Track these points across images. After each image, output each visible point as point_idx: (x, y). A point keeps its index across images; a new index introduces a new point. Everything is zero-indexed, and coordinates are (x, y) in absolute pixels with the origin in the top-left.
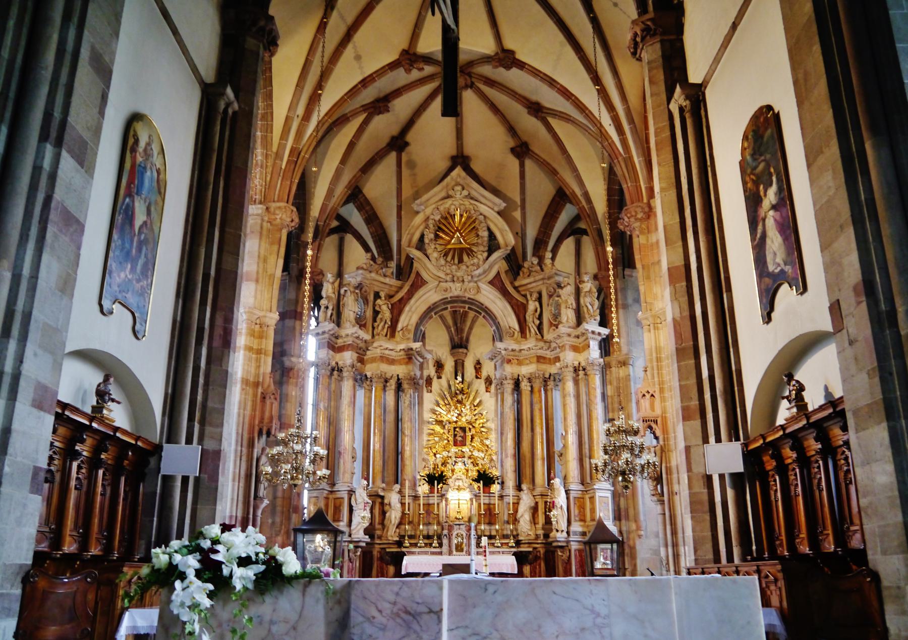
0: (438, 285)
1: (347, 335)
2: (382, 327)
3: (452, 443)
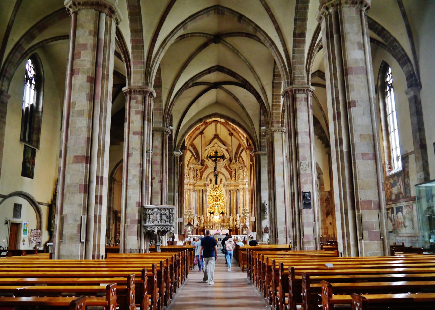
2: (198, 178)
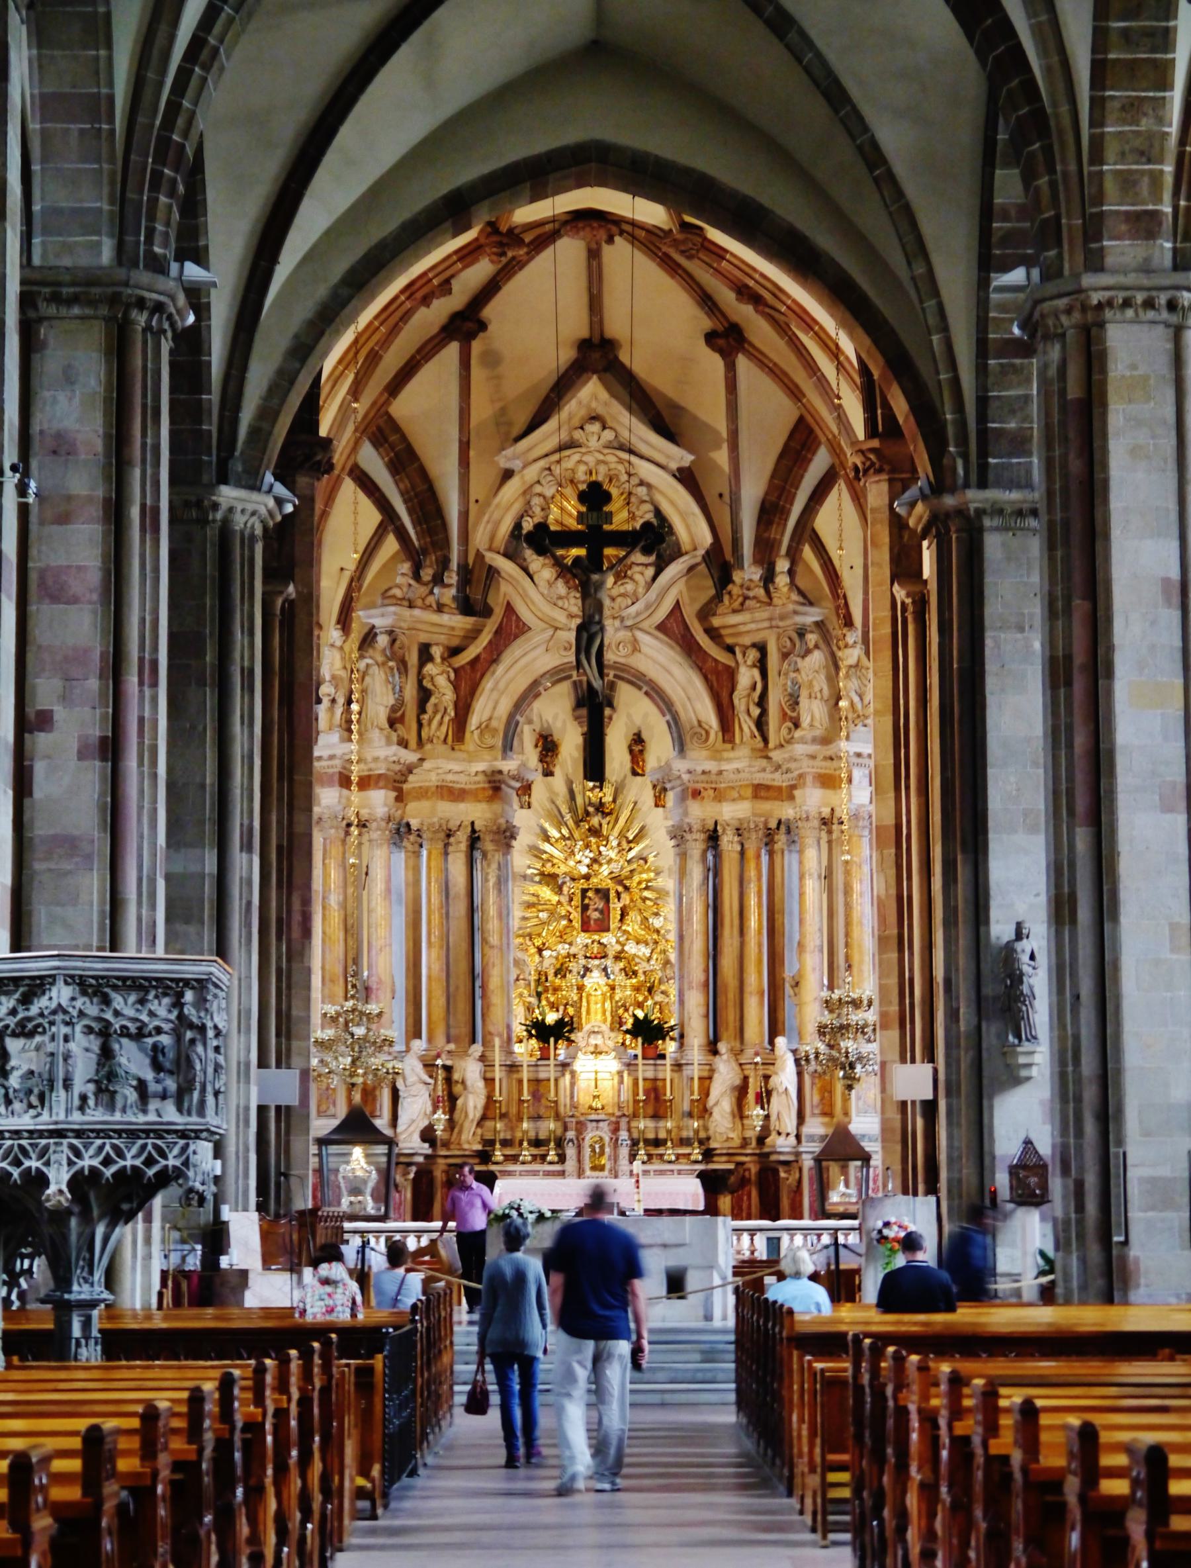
0: (553, 636)
1: (376, 759)
2: (438, 726)
3: (577, 924)
